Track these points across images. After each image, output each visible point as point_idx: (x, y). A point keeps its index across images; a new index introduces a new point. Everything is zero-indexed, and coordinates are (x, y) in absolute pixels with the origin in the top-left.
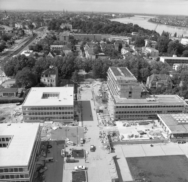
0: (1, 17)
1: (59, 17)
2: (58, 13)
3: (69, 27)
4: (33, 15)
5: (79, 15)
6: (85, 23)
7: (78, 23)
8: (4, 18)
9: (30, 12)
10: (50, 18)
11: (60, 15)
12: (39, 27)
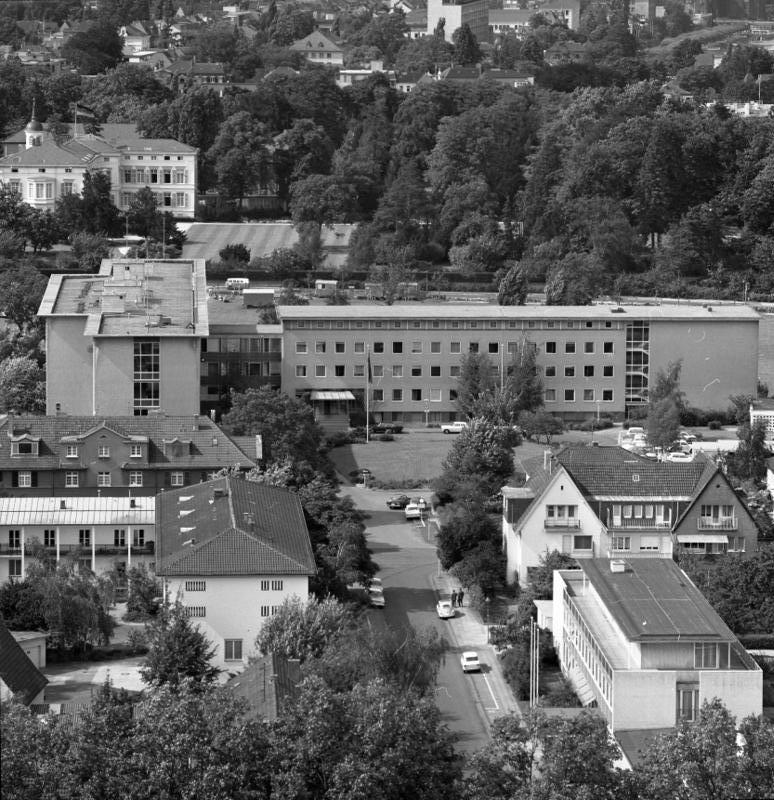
3: (147, 196)
6: (403, 109)
7: (297, 123)
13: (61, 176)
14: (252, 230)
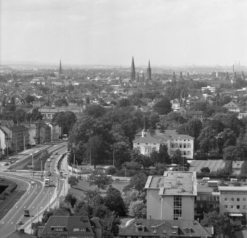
1: (113, 95)
2: (101, 76)
3: (178, 152)
5: (212, 89)
7: (225, 130)
10: (71, 104)
11: (112, 89)
12: (22, 150)
13: (152, 146)
14: (211, 163)
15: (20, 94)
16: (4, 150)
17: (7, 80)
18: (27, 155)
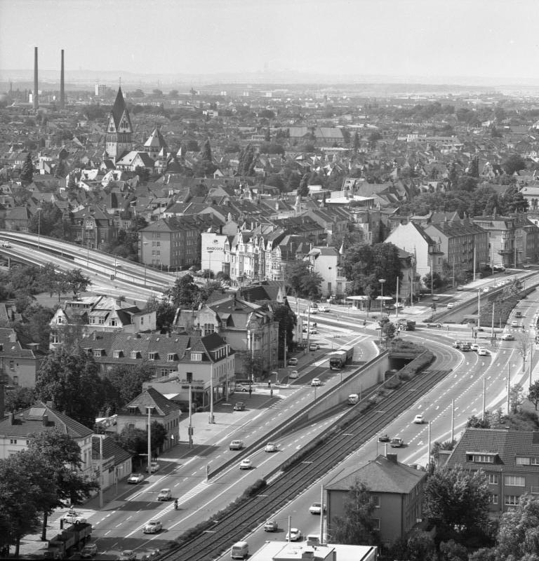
0: (69, 163)
4: (410, 138)
8: (92, 174)
9: (374, 109)
12: (470, 279)
15: (500, 154)
16: (425, 280)
17: (480, 120)
18: (477, 291)
